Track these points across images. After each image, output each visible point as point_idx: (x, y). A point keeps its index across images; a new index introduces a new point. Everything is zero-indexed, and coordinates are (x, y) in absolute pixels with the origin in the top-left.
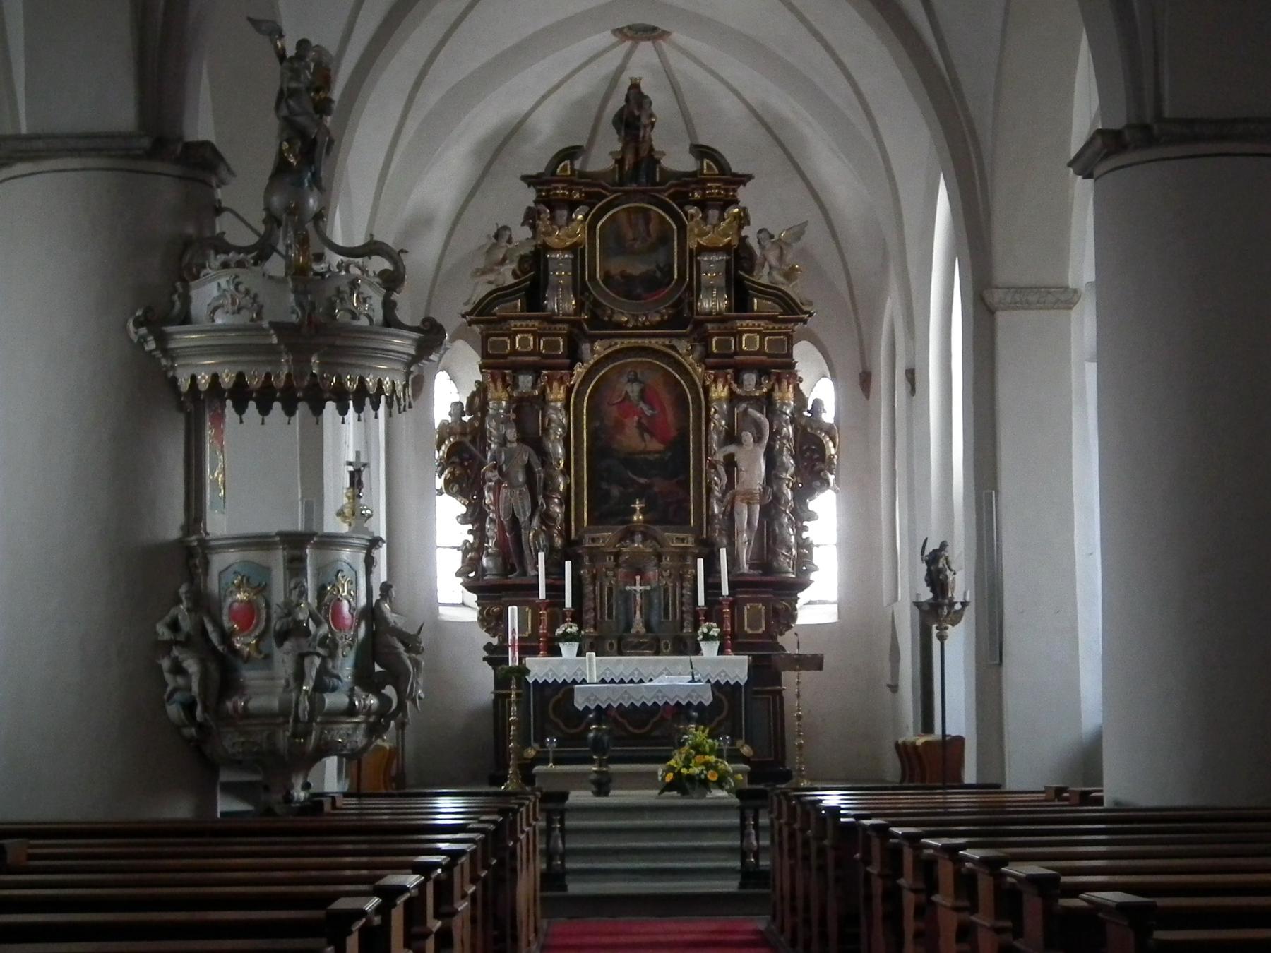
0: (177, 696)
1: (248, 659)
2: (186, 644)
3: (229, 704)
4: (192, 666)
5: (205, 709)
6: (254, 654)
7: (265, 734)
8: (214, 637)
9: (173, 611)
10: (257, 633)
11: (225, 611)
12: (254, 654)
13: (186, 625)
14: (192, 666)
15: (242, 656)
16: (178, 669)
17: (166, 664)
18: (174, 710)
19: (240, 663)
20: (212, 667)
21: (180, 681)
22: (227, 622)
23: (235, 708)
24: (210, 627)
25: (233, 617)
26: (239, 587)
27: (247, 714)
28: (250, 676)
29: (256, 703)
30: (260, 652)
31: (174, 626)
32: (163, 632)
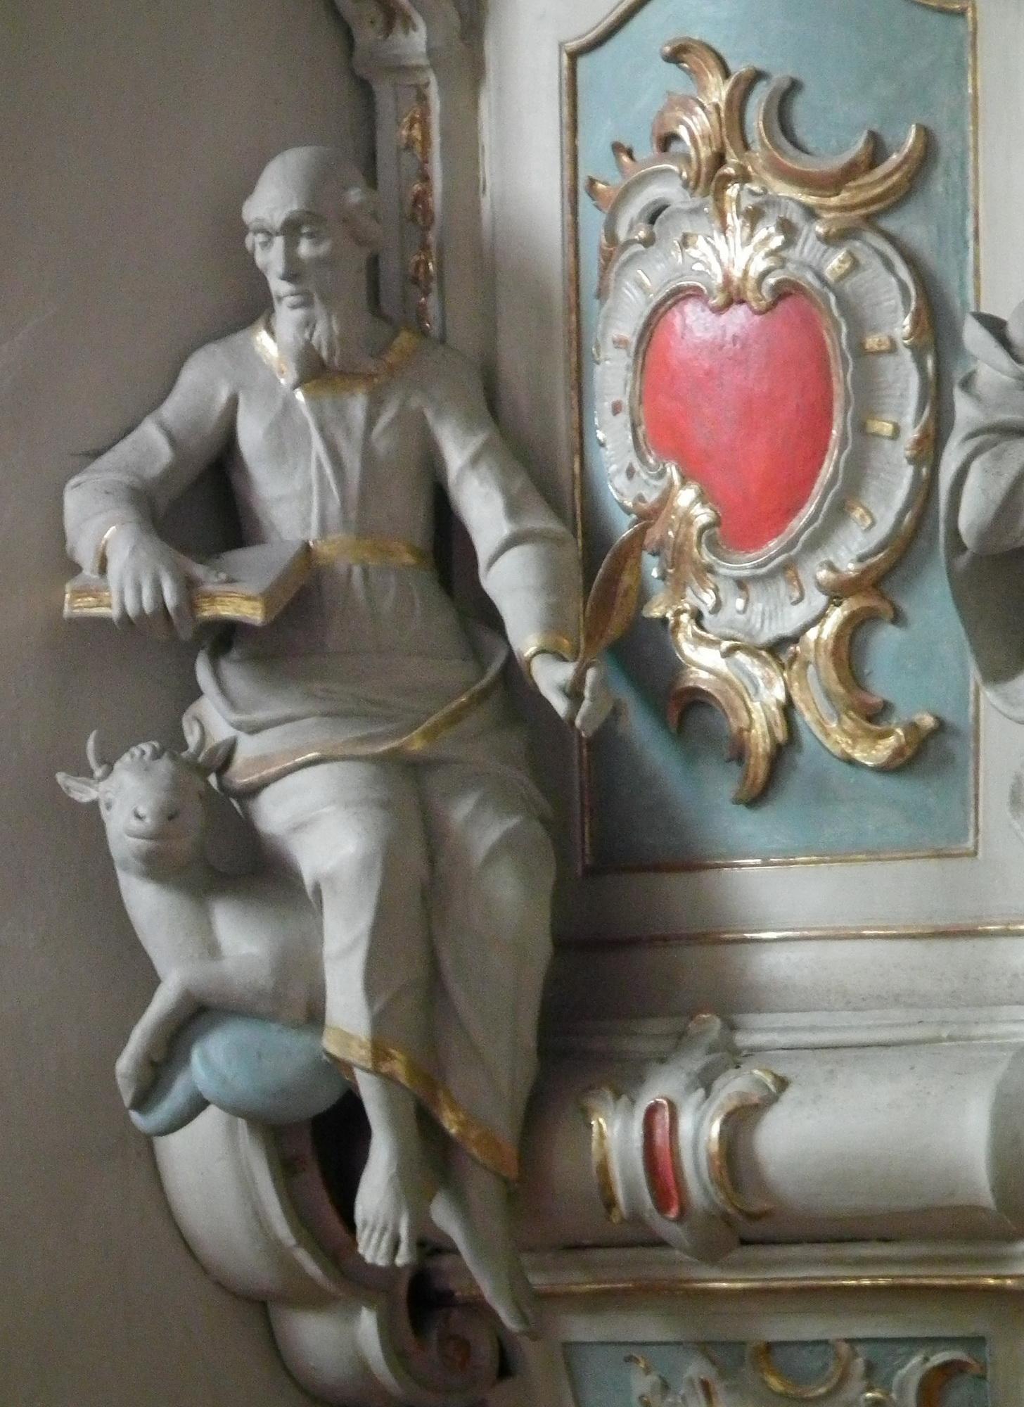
0: (213, 1060)
1: (774, 773)
2: (294, 637)
3: (615, 1132)
4: (323, 823)
5: (434, 1158)
6: (829, 731)
7: (913, 1368)
8: (515, 585)
9: (202, 382)
10: (850, 550)
11: (612, 376)
12: (829, 731)
13: (295, 497)
14: (323, 823)
15: (739, 752)
16: (227, 853)
17: (127, 799)
18: (211, 1171)
19: (710, 801)
20: (483, 827)
21: (245, 940)
22: (622, 474)
23: (659, 1163)
24: (483, 509)
25: (662, 433)
26: (712, 178)
27: (750, 1216)
28: (795, 906)
29: (806, 1136)
30: (875, 716)
31: (206, 504)
32: (115, 562)
